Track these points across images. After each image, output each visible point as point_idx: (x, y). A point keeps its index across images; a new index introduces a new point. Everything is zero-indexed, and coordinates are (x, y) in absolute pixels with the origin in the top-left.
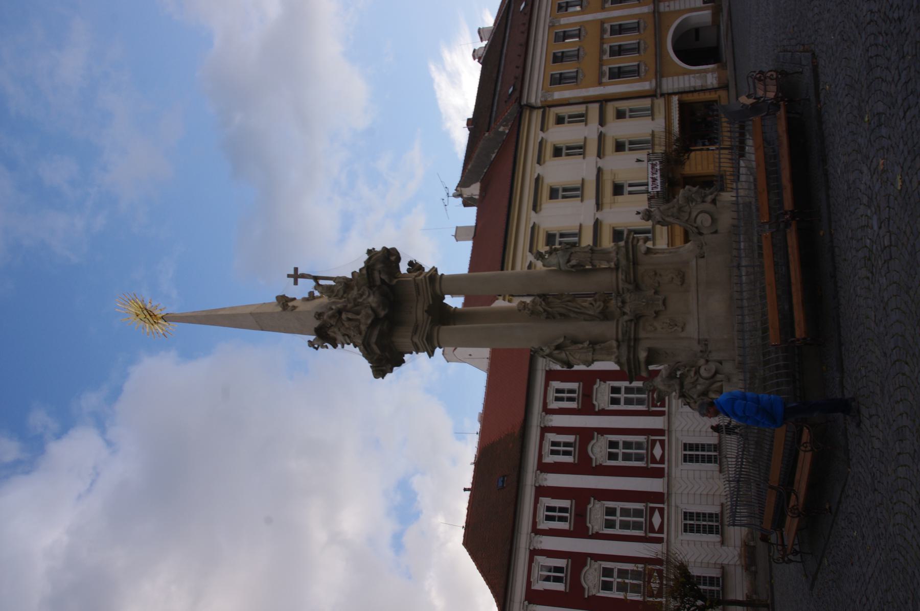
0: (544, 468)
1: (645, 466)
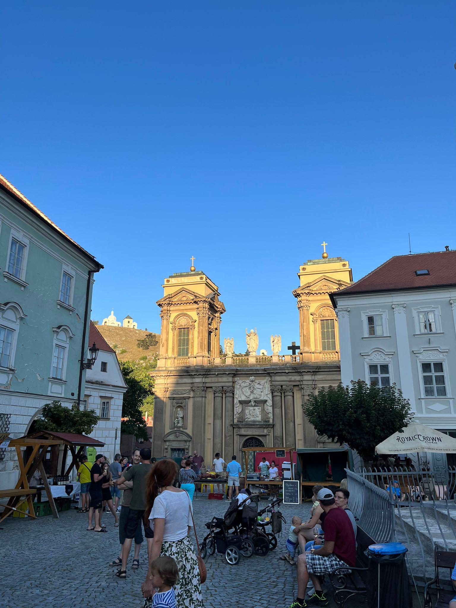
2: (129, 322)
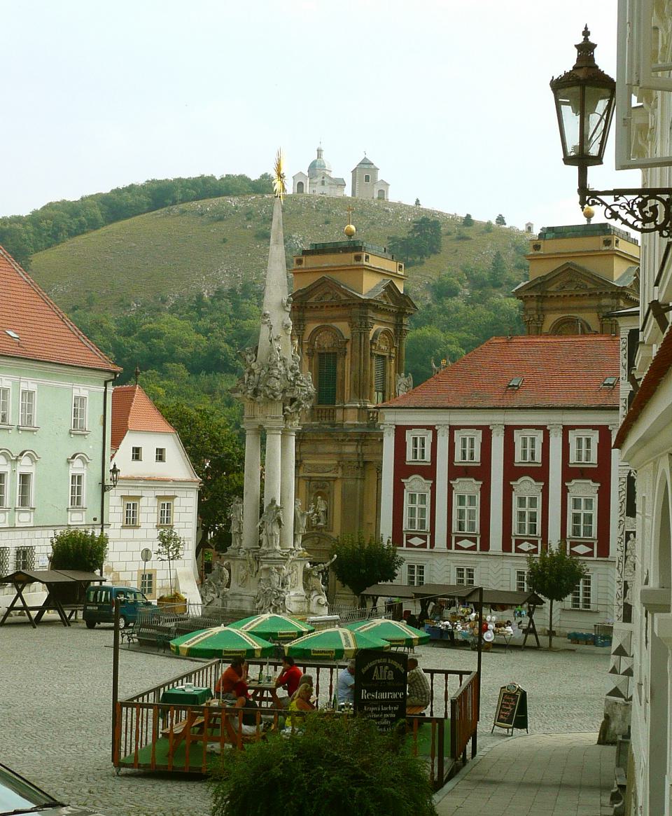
0: (509, 431)
1: (513, 534)
2: (367, 178)
